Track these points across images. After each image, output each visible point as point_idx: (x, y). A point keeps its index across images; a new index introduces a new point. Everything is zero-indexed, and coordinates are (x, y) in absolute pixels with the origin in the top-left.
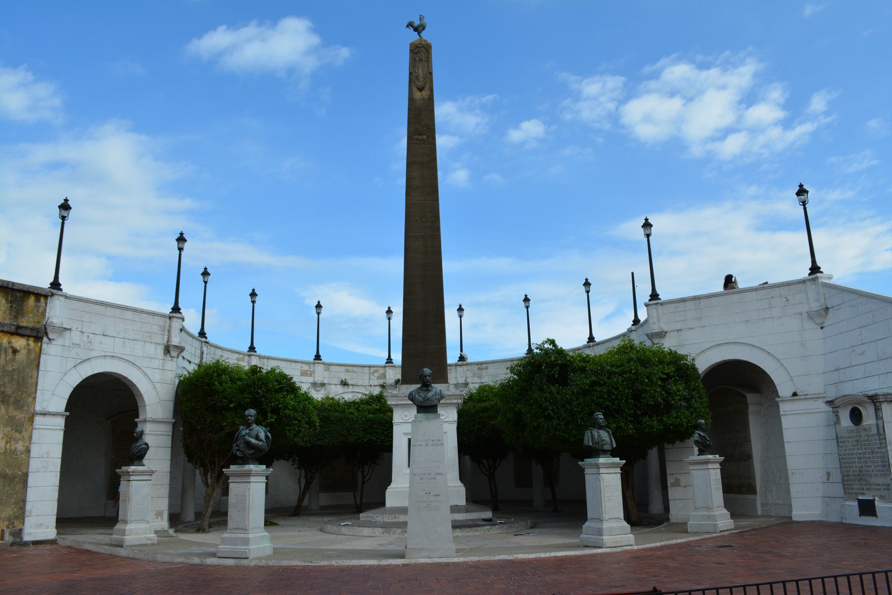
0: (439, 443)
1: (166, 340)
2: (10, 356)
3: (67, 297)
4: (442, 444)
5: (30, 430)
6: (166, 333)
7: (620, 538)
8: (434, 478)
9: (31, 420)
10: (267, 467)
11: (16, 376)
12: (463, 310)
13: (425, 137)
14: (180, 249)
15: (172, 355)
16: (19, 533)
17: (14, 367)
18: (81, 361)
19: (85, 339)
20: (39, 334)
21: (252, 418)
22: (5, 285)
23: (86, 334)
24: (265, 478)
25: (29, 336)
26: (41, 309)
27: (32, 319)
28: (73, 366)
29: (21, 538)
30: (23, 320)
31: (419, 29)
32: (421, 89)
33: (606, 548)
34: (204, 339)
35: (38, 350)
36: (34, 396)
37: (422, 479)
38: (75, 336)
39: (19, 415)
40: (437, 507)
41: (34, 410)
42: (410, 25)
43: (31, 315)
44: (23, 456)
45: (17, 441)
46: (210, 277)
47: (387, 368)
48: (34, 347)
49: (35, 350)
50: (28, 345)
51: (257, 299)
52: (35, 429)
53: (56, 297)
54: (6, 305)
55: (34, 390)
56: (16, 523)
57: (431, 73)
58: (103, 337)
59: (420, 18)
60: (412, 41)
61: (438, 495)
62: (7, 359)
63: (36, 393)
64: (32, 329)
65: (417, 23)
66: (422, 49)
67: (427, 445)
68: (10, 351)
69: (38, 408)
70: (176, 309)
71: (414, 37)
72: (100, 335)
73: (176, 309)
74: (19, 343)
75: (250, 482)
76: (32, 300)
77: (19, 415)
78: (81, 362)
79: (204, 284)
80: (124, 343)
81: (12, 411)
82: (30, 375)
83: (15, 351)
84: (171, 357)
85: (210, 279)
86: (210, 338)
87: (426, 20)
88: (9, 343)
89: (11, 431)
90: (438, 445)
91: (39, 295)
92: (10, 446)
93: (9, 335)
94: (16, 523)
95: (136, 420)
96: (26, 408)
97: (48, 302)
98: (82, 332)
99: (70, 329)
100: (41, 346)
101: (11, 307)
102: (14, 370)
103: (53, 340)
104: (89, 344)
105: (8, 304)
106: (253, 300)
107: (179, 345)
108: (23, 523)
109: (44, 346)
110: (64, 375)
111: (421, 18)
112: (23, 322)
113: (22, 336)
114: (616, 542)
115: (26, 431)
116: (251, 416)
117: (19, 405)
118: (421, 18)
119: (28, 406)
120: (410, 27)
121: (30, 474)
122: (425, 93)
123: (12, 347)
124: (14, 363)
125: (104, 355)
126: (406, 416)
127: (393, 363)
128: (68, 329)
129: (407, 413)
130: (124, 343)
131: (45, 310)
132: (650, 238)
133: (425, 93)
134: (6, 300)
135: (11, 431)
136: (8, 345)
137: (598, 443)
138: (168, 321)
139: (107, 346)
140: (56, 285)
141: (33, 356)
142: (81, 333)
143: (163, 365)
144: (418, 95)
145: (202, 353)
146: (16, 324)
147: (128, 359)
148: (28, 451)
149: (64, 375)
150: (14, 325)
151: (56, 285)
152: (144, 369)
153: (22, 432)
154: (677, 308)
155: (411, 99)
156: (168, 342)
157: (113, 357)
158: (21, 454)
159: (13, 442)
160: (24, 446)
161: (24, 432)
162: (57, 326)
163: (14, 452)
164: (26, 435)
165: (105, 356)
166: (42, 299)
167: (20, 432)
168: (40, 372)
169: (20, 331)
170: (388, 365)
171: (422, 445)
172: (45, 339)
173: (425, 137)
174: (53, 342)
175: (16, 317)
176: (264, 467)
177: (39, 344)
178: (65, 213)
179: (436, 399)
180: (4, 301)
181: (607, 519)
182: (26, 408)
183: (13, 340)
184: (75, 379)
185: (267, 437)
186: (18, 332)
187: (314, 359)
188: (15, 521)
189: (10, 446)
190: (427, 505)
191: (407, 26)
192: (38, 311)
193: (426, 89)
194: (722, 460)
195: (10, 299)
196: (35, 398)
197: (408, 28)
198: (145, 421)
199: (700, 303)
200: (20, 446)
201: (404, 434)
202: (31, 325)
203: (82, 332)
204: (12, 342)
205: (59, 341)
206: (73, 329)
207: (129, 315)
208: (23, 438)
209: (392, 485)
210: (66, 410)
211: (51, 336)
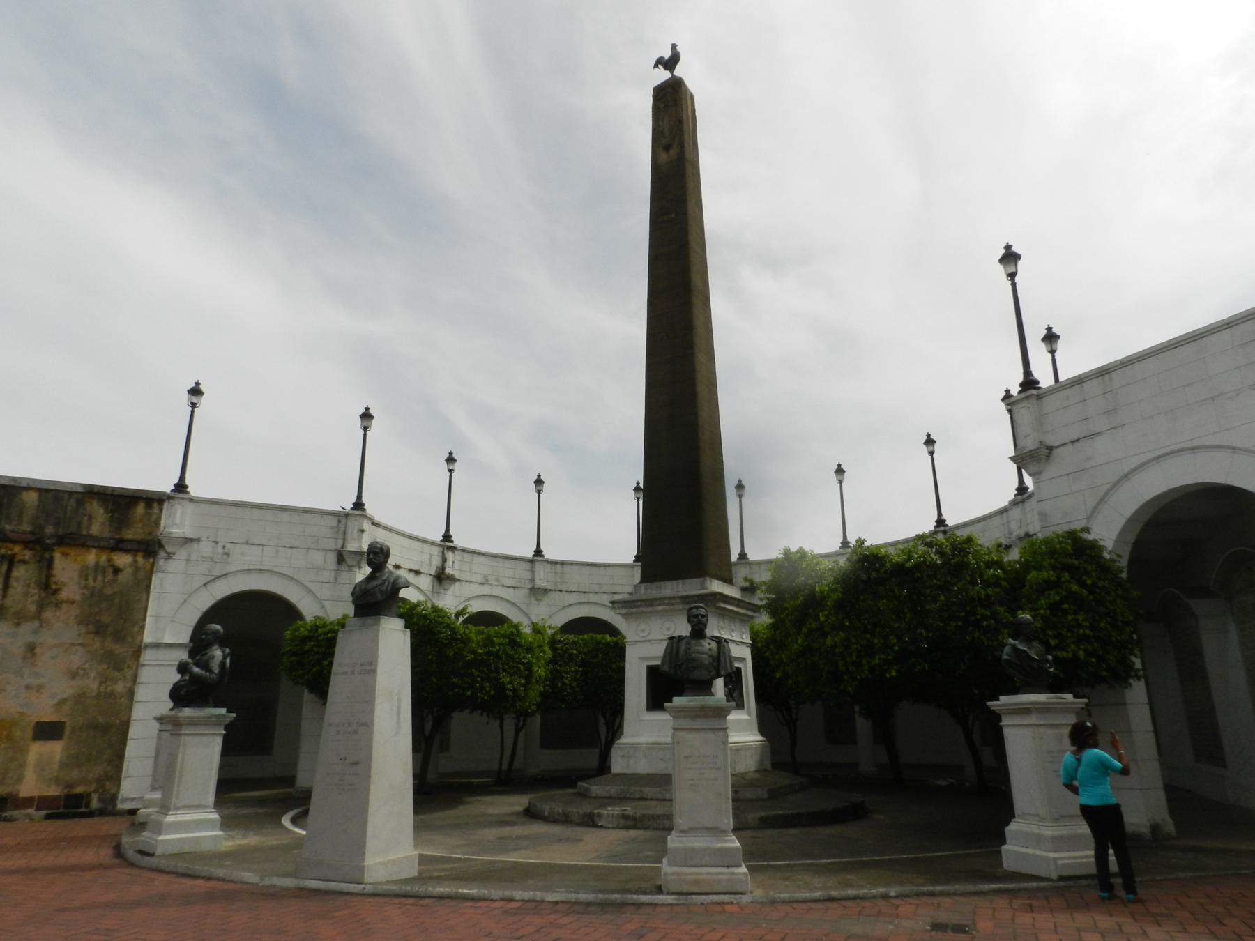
0: (369, 668)
1: (340, 542)
2: (110, 577)
3: (191, 500)
4: (374, 671)
5: (134, 667)
6: (341, 536)
7: (708, 874)
8: (356, 732)
9: (137, 653)
10: (227, 712)
11: (116, 601)
12: (844, 471)
13: (673, 216)
14: (365, 429)
15: (349, 563)
16: (114, 798)
17: (115, 590)
18: (213, 577)
19: (220, 550)
20: (151, 548)
21: (209, 637)
22: (102, 491)
23: (221, 545)
24: (223, 728)
25: (138, 551)
26: (154, 517)
27: (141, 531)
28: (202, 584)
29: (115, 805)
30: (128, 531)
32: (667, 148)
33: (668, 894)
34: (447, 544)
35: (148, 566)
36: (141, 624)
37: (338, 732)
38: (205, 548)
39: (119, 649)
40: (352, 785)
41: (141, 641)
42: (660, 62)
43: (140, 525)
44: (123, 699)
45: (115, 681)
46: (456, 464)
48: (144, 564)
49: (145, 568)
50: (135, 561)
51: (545, 487)
52: (143, 665)
53: (177, 501)
54: (105, 515)
55: (142, 617)
56: (108, 785)
57: (680, 122)
58: (247, 546)
59: (672, 48)
61: (356, 763)
62: (106, 580)
63: (144, 620)
64: (139, 542)
65: (667, 54)
67: (353, 672)
68: (110, 570)
69: (147, 638)
70: (359, 505)
71: (663, 75)
72: (243, 543)
73: (359, 505)
74: (122, 560)
75: (180, 735)
76: (140, 509)
77: (119, 649)
78: (215, 579)
79: (449, 473)
80: (277, 552)
81: (110, 644)
82: (137, 598)
83: (117, 571)
84: (348, 566)
85: (456, 467)
86: (458, 541)
88: (109, 560)
89: (109, 667)
90: (367, 672)
91: (153, 500)
92: (106, 688)
93: (109, 551)
94: (108, 785)
96: (130, 640)
97: (164, 511)
98: (214, 542)
99: (198, 540)
100: (154, 562)
101: (112, 516)
102: (114, 594)
103: (174, 554)
104: (225, 557)
105: (108, 513)
106: (539, 488)
107: (359, 550)
108: (119, 786)
109: (161, 562)
110: (189, 597)
111: (674, 47)
112: (129, 534)
113: (127, 551)
114: (696, 882)
115: (128, 667)
116: (206, 634)
117: (119, 637)
118: (674, 47)
119: (133, 638)
120: (660, 66)
121: (132, 723)
123: (113, 566)
124: (115, 585)
125: (247, 568)
126: (643, 631)
128: (195, 540)
129: (643, 626)
130: (277, 552)
131: (159, 518)
132: (1017, 279)
134: (106, 511)
135: (109, 667)
136: (106, 564)
137: (680, 666)
138: (344, 521)
139: (252, 557)
140: (181, 487)
141: (141, 575)
142: (214, 544)
143: (336, 579)
144: (664, 157)
146: (118, 537)
147: (282, 572)
148: (131, 694)
149: (189, 597)
150: (114, 539)
151: (181, 487)
152: (308, 584)
153: (123, 669)
154: (1067, 398)
156: (342, 547)
157: (261, 570)
158: (121, 698)
159: (109, 683)
160: (125, 687)
161: (126, 670)
162: (177, 536)
163: (111, 695)
164: (129, 673)
165: (249, 570)
166: (155, 505)
167: (119, 669)
168: (152, 595)
169: (121, 546)
170: (743, 561)
171: (345, 673)
172: (162, 554)
173: (673, 216)
174: (174, 557)
175: (119, 529)
176: (223, 711)
177: (151, 560)
178: (194, 400)
179: (381, 592)
180: (102, 511)
181: (685, 827)
182: (130, 640)
183: (115, 558)
184: (206, 600)
185: (222, 664)
186: (119, 546)
187: (634, 561)
188: (108, 783)
189: (106, 688)
190: (341, 780)
191: (656, 66)
192: (149, 520)
194: (1083, 706)
195: (110, 507)
196: (143, 627)
197: (656, 69)
199: (1111, 379)
200: (120, 688)
201: (641, 658)
202: (138, 537)
203: (214, 542)
204: (113, 560)
205: (182, 554)
206: (203, 539)
207: (285, 516)
208: (125, 677)
209: (623, 740)
210: (192, 640)
211: (169, 549)
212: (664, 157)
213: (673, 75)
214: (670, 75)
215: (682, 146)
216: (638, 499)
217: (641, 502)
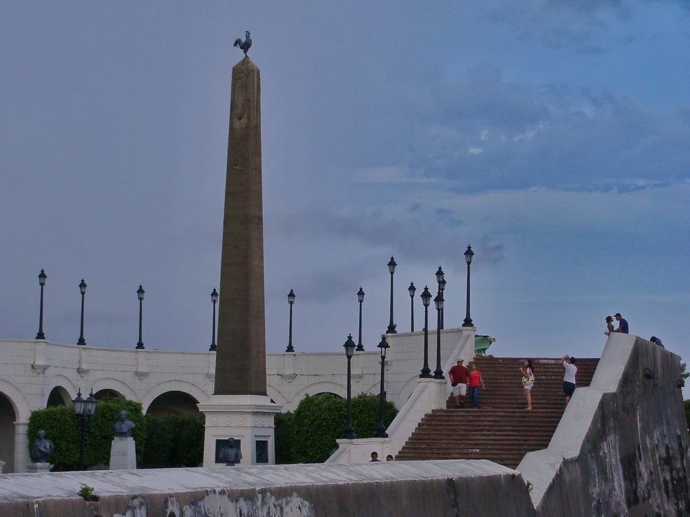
0: (124, 454)
14: (42, 284)
31: (246, 46)
42: (237, 42)
47: (286, 356)
51: (145, 296)
60: (235, 63)
65: (244, 40)
66: (242, 74)
87: (251, 37)
95: (14, 423)
106: (141, 296)
111: (248, 34)
118: (248, 34)
122: (244, 121)
127: (294, 351)
133: (244, 121)
145: (81, 358)
155: (232, 129)
185: (51, 447)
187: (210, 350)
191: (235, 45)
193: (245, 117)
198: (18, 424)
212: (238, 124)
213: (246, 56)
214: (244, 56)
215: (249, 118)
216: (214, 302)
217: (217, 305)
